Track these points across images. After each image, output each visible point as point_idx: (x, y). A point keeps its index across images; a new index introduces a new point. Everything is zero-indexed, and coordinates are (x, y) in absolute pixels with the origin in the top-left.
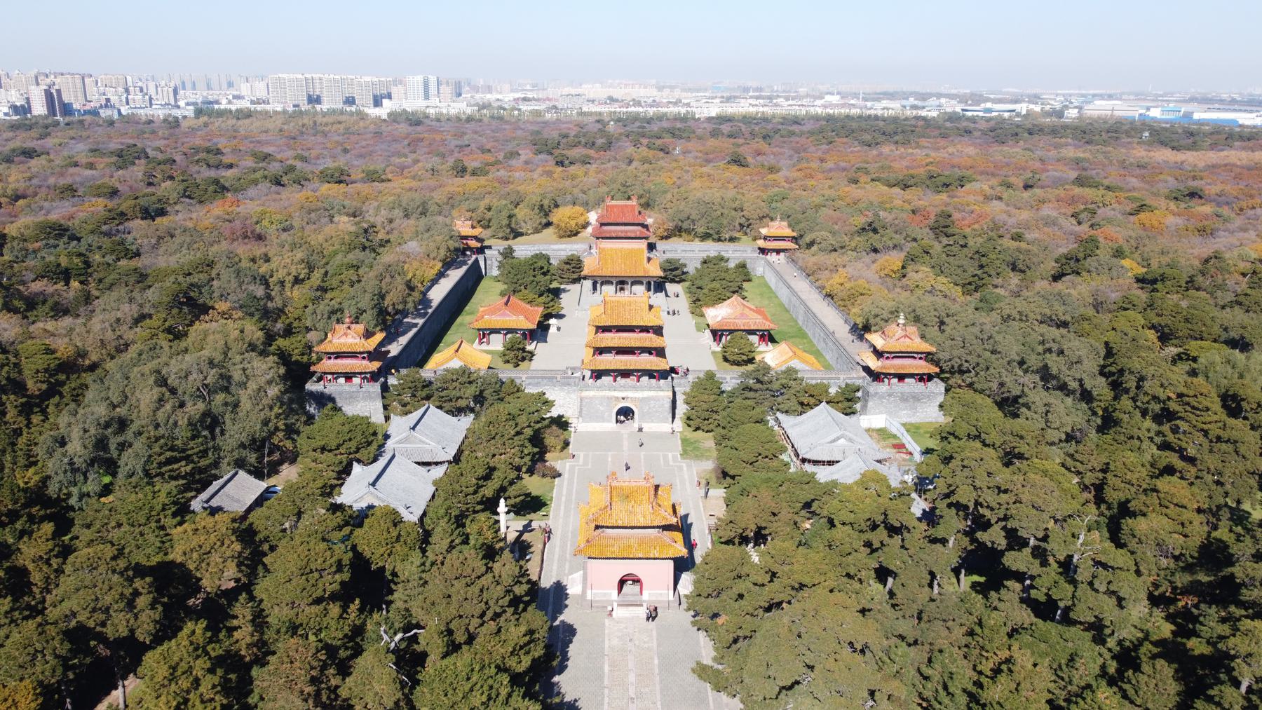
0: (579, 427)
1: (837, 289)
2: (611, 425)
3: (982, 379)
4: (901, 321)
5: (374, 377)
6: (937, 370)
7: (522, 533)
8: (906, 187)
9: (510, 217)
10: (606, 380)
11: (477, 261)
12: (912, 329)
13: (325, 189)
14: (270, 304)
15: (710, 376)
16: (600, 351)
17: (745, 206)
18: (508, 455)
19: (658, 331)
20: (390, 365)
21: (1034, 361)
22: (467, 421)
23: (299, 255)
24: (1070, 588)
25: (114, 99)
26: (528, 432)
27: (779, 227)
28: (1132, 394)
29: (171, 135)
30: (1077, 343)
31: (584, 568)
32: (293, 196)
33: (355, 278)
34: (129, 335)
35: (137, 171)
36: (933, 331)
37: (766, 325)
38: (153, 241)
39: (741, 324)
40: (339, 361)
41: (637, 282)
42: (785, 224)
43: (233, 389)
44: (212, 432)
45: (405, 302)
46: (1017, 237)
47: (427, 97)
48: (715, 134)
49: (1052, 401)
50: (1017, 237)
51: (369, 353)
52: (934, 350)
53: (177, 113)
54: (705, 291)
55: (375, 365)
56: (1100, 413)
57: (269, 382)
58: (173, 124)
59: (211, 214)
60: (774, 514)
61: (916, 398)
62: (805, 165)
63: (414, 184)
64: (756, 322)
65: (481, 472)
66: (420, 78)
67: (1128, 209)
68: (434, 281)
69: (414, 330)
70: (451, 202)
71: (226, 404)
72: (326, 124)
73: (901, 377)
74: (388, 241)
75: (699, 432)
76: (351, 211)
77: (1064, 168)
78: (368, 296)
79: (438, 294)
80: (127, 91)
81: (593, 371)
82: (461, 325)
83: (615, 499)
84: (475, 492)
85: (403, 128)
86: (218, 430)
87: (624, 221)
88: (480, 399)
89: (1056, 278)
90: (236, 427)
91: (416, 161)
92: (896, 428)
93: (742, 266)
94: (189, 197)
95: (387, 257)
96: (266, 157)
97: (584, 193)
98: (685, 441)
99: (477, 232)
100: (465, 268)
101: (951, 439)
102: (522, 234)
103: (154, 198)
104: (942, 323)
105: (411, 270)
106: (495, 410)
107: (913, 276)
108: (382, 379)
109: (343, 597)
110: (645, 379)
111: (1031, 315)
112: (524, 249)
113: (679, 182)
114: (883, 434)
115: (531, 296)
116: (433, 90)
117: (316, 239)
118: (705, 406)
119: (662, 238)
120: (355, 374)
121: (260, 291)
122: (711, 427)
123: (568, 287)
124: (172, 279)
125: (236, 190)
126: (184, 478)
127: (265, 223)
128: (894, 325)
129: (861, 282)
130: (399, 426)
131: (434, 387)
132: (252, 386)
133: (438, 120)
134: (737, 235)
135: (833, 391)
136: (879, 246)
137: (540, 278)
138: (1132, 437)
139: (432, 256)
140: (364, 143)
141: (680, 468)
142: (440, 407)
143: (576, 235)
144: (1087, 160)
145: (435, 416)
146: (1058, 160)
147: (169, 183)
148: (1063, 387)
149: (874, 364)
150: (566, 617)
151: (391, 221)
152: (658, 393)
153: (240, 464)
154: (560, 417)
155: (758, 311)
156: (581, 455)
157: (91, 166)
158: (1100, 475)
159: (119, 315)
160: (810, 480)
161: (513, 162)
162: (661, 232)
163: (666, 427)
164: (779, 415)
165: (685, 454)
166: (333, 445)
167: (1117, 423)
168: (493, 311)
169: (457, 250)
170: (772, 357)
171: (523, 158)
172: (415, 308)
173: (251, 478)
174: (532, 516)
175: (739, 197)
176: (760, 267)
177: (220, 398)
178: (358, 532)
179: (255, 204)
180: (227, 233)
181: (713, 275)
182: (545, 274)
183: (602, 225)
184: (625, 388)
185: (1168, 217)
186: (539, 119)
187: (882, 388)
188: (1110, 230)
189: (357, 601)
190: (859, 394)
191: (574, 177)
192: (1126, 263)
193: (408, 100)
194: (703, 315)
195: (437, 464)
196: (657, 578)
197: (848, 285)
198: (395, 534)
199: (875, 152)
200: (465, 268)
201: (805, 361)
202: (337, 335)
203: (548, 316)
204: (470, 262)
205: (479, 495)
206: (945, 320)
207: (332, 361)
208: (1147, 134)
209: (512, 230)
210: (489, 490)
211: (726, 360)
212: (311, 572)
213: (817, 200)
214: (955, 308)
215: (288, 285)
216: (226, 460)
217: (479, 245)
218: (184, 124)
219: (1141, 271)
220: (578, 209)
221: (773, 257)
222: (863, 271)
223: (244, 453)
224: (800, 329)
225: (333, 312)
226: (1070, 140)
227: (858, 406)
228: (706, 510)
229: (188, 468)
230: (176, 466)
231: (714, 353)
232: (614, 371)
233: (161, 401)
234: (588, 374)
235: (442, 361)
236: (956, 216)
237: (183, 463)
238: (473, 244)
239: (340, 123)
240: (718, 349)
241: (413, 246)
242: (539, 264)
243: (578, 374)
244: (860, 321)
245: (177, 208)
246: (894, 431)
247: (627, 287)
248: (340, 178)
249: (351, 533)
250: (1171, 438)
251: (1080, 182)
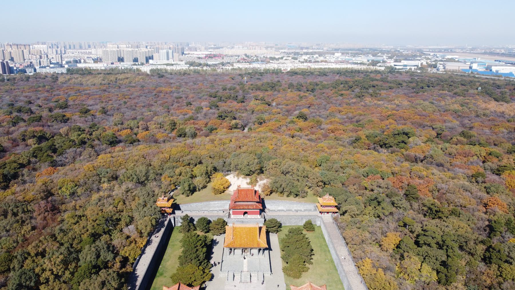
8: (384, 145)
11: (170, 220)
25: (34, 62)
47: (168, 59)
53: (59, 70)
58: (55, 77)
62: (333, 119)
66: (165, 51)
72: (121, 80)
80: (41, 57)
87: (247, 199)
91: (156, 114)
94: (36, 157)
100: (163, 230)
113: (275, 147)
127: (64, 189)
133: (171, 74)
140: (136, 94)
143: (223, 192)
162: (266, 192)
186: (215, 73)
193: (159, 62)
199: (363, 103)
200: (163, 230)
204: (166, 223)
208: (480, 88)
213: (343, 163)
218: (61, 79)
226: (447, 92)
239: (127, 78)
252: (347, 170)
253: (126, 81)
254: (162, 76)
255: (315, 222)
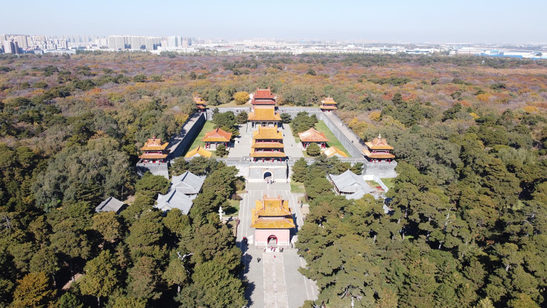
0: (249, 181)
1: (353, 125)
2: (262, 180)
3: (412, 160)
4: (380, 137)
5: (164, 160)
6: (394, 157)
7: (228, 221)
8: (382, 83)
9: (217, 96)
10: (260, 161)
11: (203, 114)
12: (384, 140)
13: (137, 84)
14: (119, 132)
15: (302, 159)
16: (257, 149)
17: (315, 91)
18: (221, 191)
19: (281, 141)
20: (171, 156)
21: (433, 152)
22: (203, 178)
23: (130, 111)
24: (444, 236)
25: (40, 46)
26: (229, 182)
27: (329, 100)
28: (471, 165)
29: (67, 62)
30: (450, 145)
31: (254, 234)
32: (123, 88)
33: (155, 121)
34: (62, 144)
35: (55, 77)
36: (393, 141)
37: (324, 140)
38: (67, 106)
39: (314, 139)
40: (150, 154)
41: (270, 122)
42: (332, 99)
43: (108, 165)
44: (101, 182)
45: (175, 131)
46: (428, 104)
47: (177, 45)
48: (301, 61)
49: (440, 168)
50: (428, 104)
51: (163, 150)
52: (393, 148)
53: (68, 52)
54: (299, 126)
55: (165, 156)
56: (459, 172)
57: (124, 162)
58: (67, 57)
59: (89, 95)
60: (329, 212)
61: (386, 168)
63: (175, 82)
64: (320, 138)
65: (211, 196)
66: (174, 37)
67: (474, 93)
68: (186, 123)
69: (180, 142)
70: (191, 90)
71: (106, 171)
72: (134, 57)
73: (380, 160)
74: (166, 106)
75: (298, 183)
76: (149, 94)
77: (448, 76)
78: (161, 128)
79: (188, 127)
80: (46, 42)
81: (254, 158)
82: (198, 140)
83: (266, 205)
84: (209, 205)
85: (167, 59)
86: (103, 181)
88: (208, 169)
89: (443, 120)
90: (110, 180)
92: (377, 180)
93: (314, 116)
94: (79, 88)
95: (166, 112)
96: (109, 71)
97: (247, 86)
98: (292, 186)
99: (203, 102)
100: (198, 117)
101: (399, 182)
102: (221, 103)
103: (64, 88)
104: (396, 138)
105: (177, 117)
106: (216, 173)
107: (385, 120)
108: (168, 162)
109: (160, 243)
110: (276, 161)
111: (433, 135)
112: (223, 109)
113: (287, 82)
114: (372, 182)
115: (227, 129)
116: (179, 43)
117: (136, 105)
118: (300, 172)
119: (280, 105)
120: (157, 159)
121: (115, 127)
122: (303, 180)
123: (242, 125)
124: (78, 121)
125: (99, 85)
126: (90, 200)
127: (113, 99)
128: (377, 139)
129: (363, 122)
130: (176, 180)
131: (189, 164)
132: (117, 163)
133: (182, 55)
134: (312, 103)
135: (352, 165)
136: (371, 108)
137: (230, 121)
138: (471, 182)
139: (185, 112)
140: (151, 65)
141: (291, 196)
142: (192, 172)
143: (244, 103)
144: (458, 73)
145: (191, 176)
146: (446, 72)
147: (69, 82)
148: (444, 163)
149: (369, 154)
150: (248, 252)
151: (166, 98)
152: (281, 167)
153: (112, 195)
154: (242, 177)
155: (321, 134)
156: (250, 192)
157: (35, 75)
158: (458, 196)
159: (57, 136)
160: (343, 199)
161: (216, 73)
162: (280, 102)
163: (284, 180)
164: (330, 175)
165: (292, 191)
166: (150, 187)
167: (465, 176)
168: (211, 135)
169: (195, 109)
170: (328, 152)
171: (220, 72)
172: (179, 133)
173: (117, 201)
174: (232, 215)
175: (312, 87)
176: (321, 117)
177: (104, 168)
178: (165, 219)
179: (108, 91)
180: (98, 103)
181: (302, 120)
182: (232, 119)
183: (256, 99)
184: (267, 165)
185: (491, 96)
186: (226, 55)
187: (372, 164)
188: (466, 101)
189: (166, 245)
190: (363, 167)
191: (242, 80)
192: (472, 114)
194: (298, 136)
195: (193, 194)
196: (283, 236)
197: (358, 124)
198: (179, 219)
199: (369, 69)
201: (340, 154)
202: (149, 143)
203: (234, 137)
205: (211, 205)
206: (398, 137)
207: (147, 154)
208: (483, 61)
209: (218, 102)
210: (215, 204)
211: (308, 154)
212: (148, 233)
213: (345, 89)
214: (401, 132)
215: (126, 124)
216: (107, 193)
217: (204, 108)
218: (72, 57)
219: (478, 117)
220: (245, 93)
221: (327, 113)
222: (364, 118)
223: (114, 190)
224: (338, 142)
225: (146, 135)
227: (362, 172)
228: (302, 212)
229: (92, 196)
230: (87, 195)
231: (303, 151)
232: (263, 158)
233: (80, 169)
234: (252, 159)
235: (191, 155)
236: (403, 95)
237: (90, 194)
238: (202, 107)
239: (140, 56)
240: (305, 150)
241: (176, 108)
242: (230, 115)
243: (248, 159)
244: (363, 138)
245: (75, 92)
246: (377, 181)
247: (267, 125)
248: (143, 80)
249: (162, 219)
250: (487, 182)
251: (455, 81)
252: (348, 94)
253: (138, 58)
254: (174, 57)
255: (319, 118)
